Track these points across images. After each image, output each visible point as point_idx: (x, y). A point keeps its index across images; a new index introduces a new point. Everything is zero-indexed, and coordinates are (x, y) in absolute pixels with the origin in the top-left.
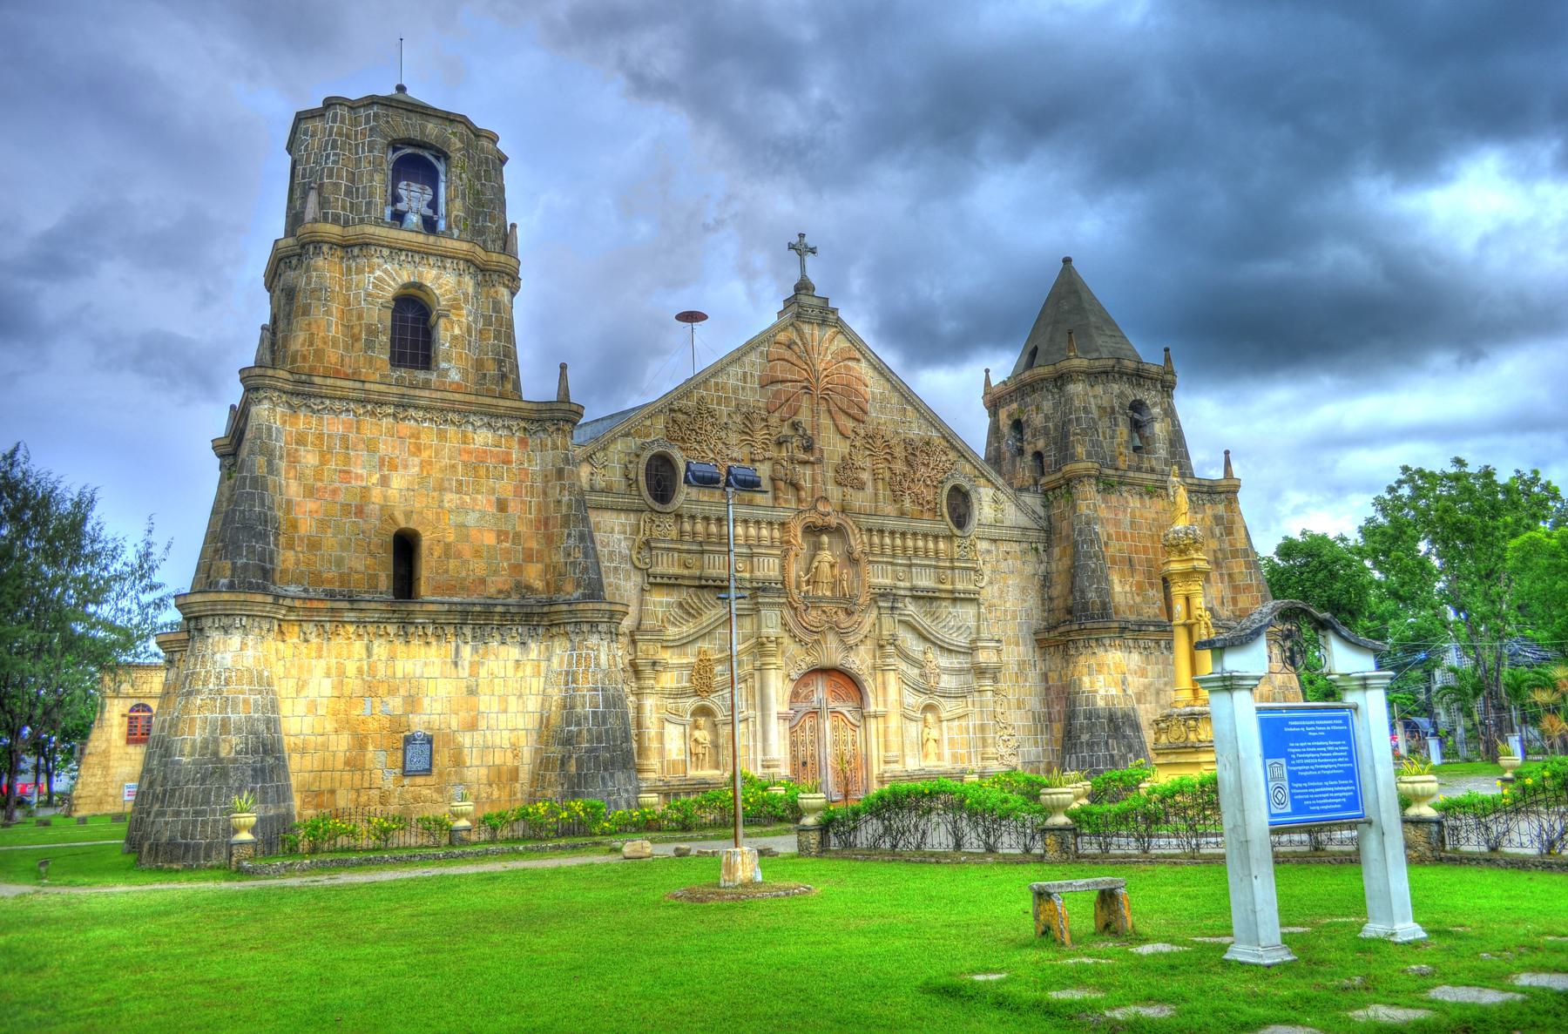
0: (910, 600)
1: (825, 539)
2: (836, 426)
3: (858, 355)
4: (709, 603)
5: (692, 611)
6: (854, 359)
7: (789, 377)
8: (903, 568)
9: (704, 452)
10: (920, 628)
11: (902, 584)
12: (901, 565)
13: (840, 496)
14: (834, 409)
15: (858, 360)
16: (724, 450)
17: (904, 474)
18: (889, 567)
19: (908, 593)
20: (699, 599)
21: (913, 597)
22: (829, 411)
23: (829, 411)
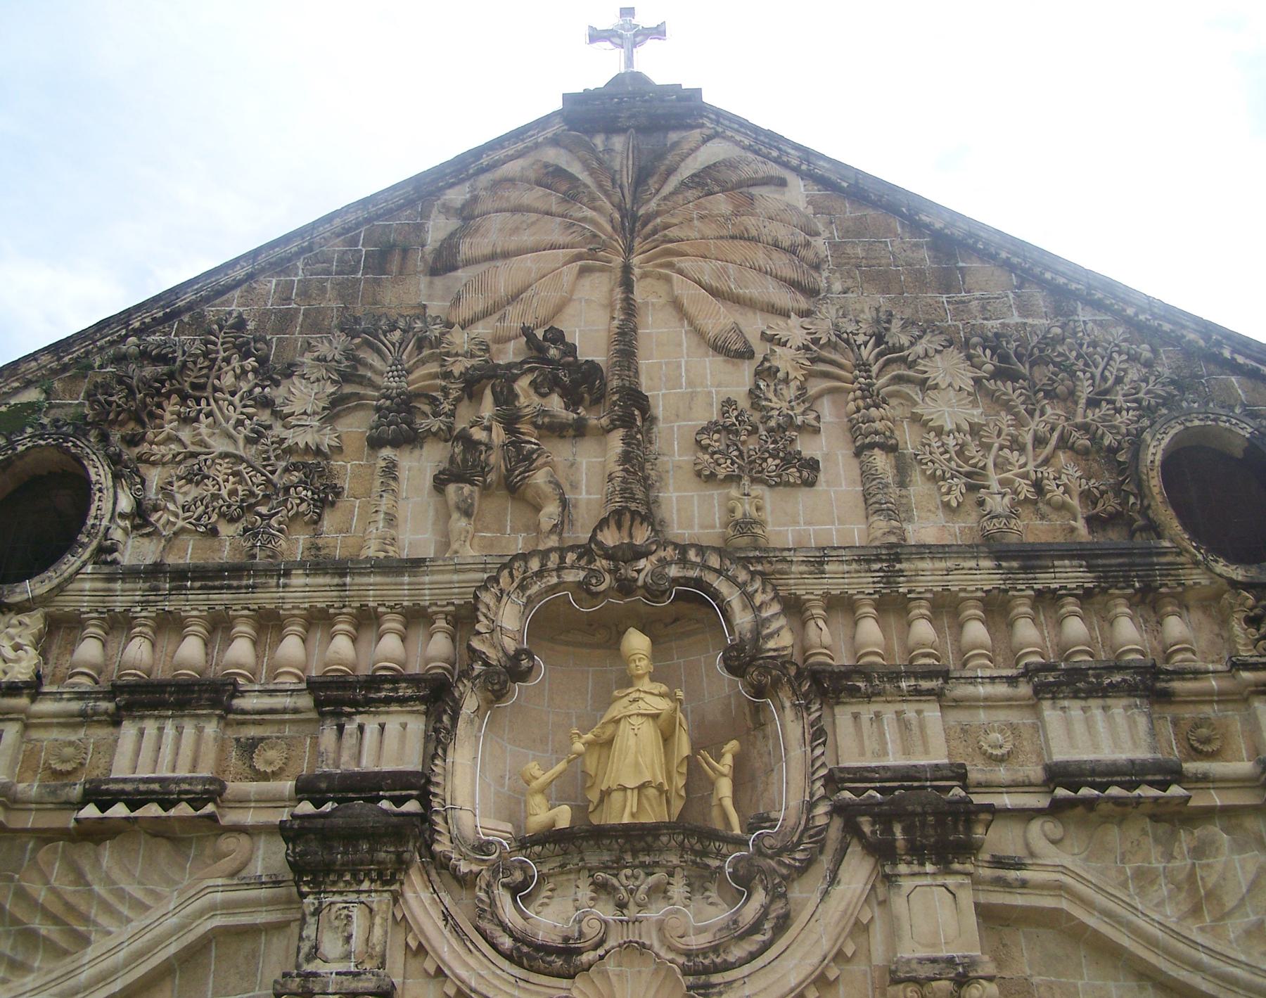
0: (1052, 828)
1: (637, 642)
2: (699, 333)
3: (775, 170)
4: (121, 894)
5: (45, 929)
6: (767, 181)
7: (527, 239)
8: (1002, 716)
9: (202, 443)
10: (1125, 941)
11: (1002, 774)
12: (990, 703)
13: (717, 517)
14: (686, 290)
15: (782, 183)
16: (278, 430)
17: (975, 430)
18: (932, 712)
19: (1041, 801)
20: (80, 878)
21: (1056, 809)
22: (677, 305)
23: (677, 305)
